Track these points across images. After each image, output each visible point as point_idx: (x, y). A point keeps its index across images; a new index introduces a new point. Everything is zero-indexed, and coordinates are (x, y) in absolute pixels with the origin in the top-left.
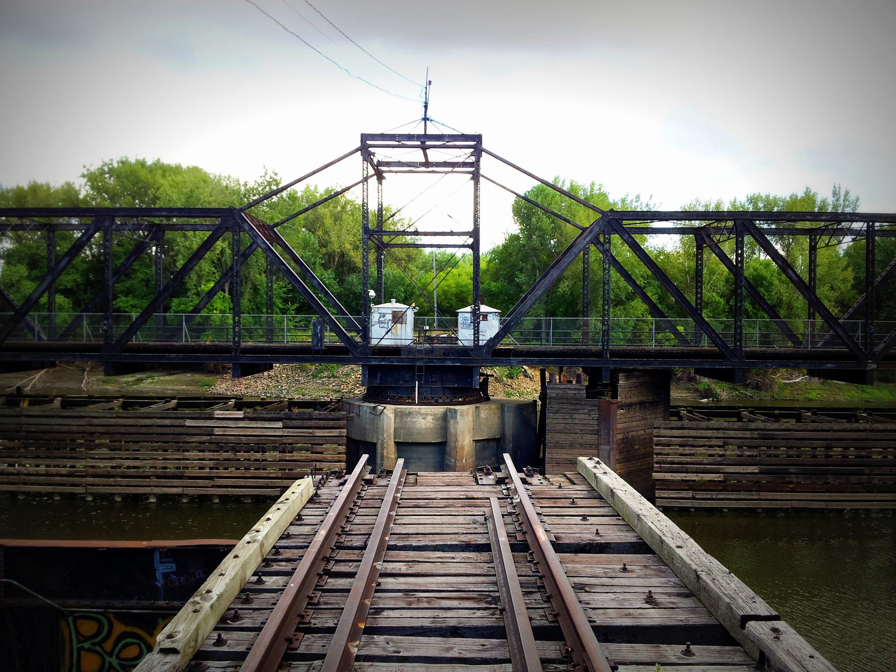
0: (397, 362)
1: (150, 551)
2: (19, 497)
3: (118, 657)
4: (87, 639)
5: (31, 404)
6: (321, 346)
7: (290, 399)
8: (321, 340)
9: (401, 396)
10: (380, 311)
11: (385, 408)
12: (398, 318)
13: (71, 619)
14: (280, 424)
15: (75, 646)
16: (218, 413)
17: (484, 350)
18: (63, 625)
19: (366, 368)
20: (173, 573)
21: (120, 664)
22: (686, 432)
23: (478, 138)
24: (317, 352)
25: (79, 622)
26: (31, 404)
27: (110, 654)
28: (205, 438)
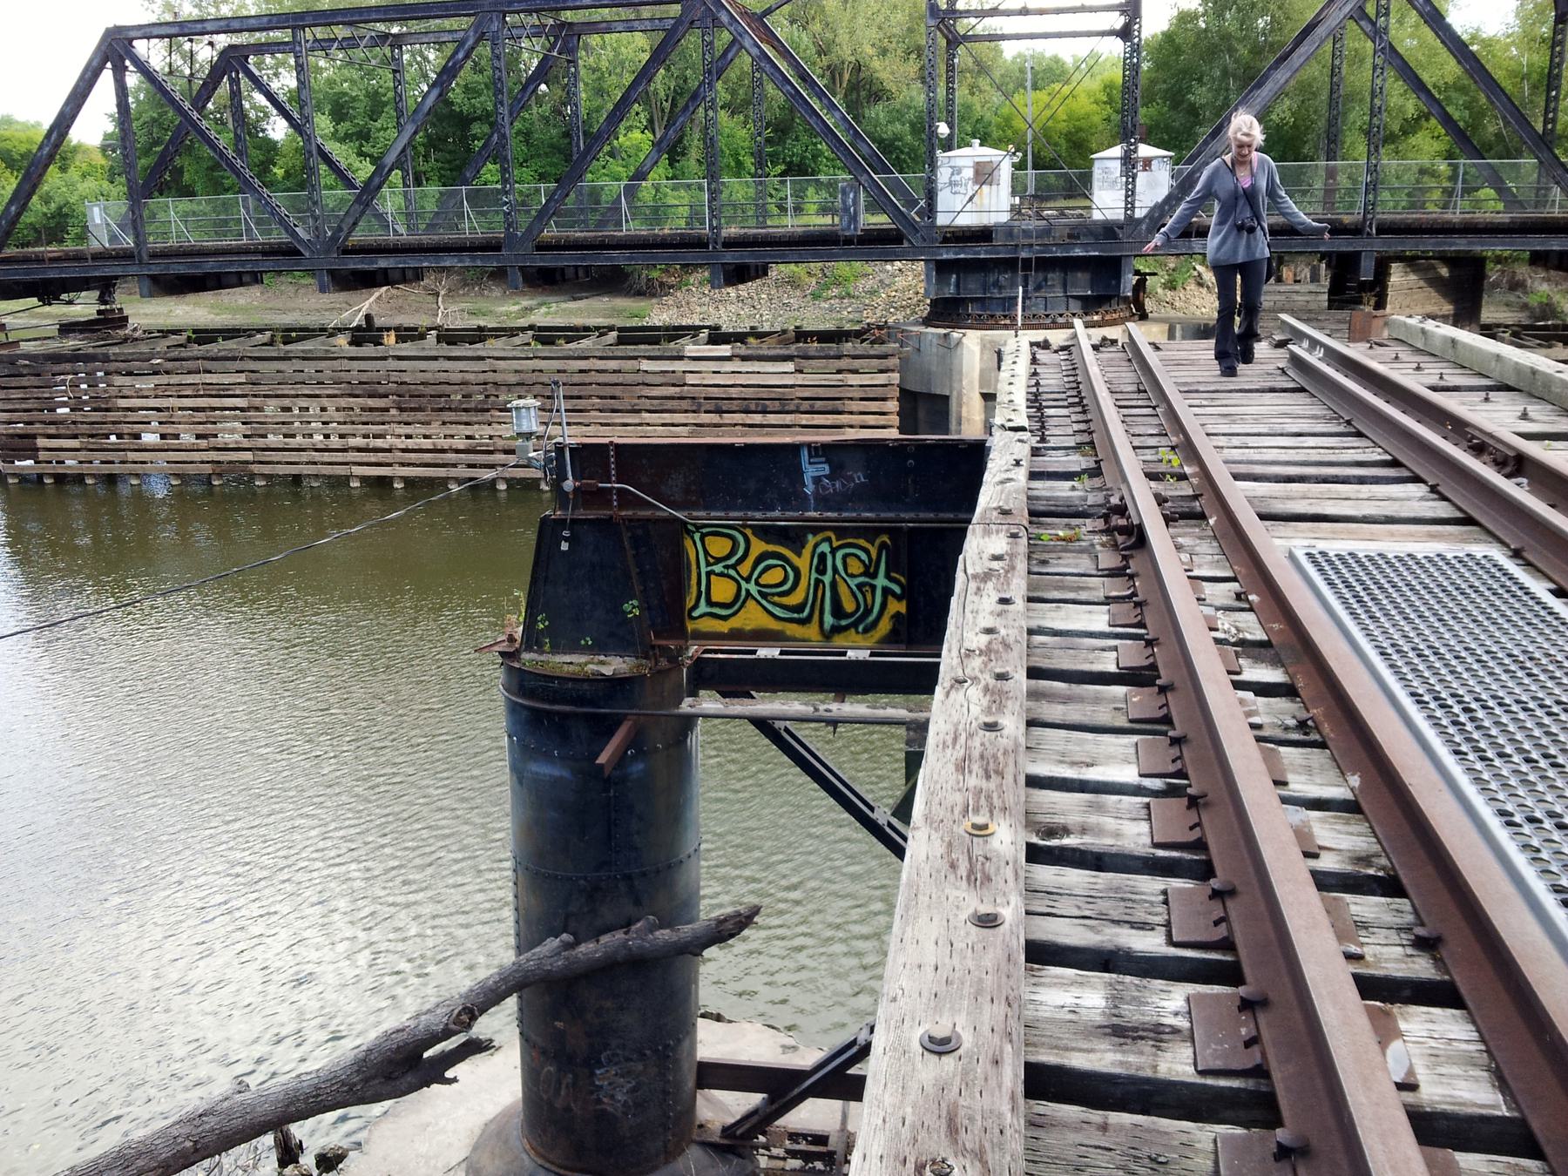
0: (986, 252)
1: (795, 449)
2: (396, 485)
3: (757, 583)
4: (718, 560)
5: (401, 339)
6: (855, 229)
7: (797, 327)
8: (854, 218)
9: (994, 314)
10: (952, 164)
11: (964, 335)
12: (984, 175)
13: (697, 536)
15: (704, 570)
16: (691, 349)
17: (1144, 227)
18: (688, 543)
19: (932, 265)
20: (825, 476)
21: (759, 592)
24: (848, 241)
25: (707, 539)
26: (401, 339)
27: (748, 580)
28: (672, 391)
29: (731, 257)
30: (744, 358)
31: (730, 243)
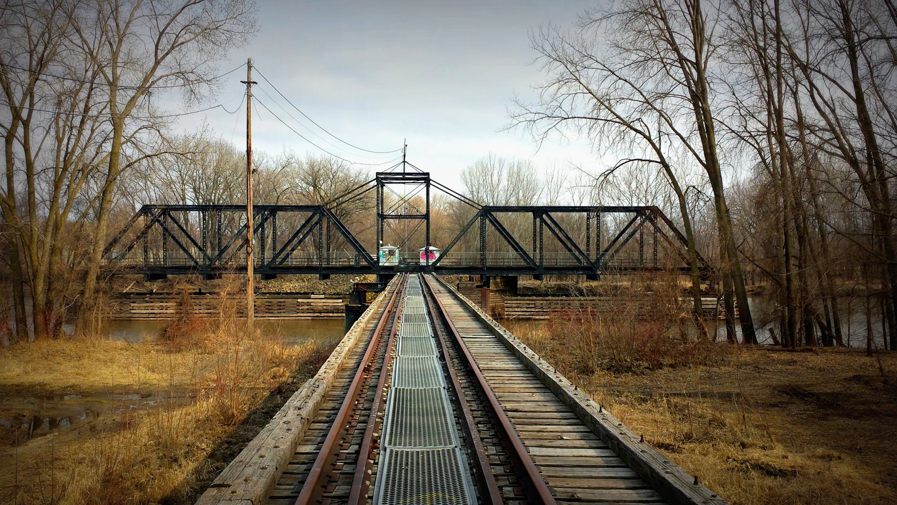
8: (358, 263)
12: (391, 253)
14: (341, 301)
16: (313, 296)
22: (518, 302)
23: (428, 174)
24: (357, 269)
29: (324, 272)
30: (327, 298)
31: (325, 269)
